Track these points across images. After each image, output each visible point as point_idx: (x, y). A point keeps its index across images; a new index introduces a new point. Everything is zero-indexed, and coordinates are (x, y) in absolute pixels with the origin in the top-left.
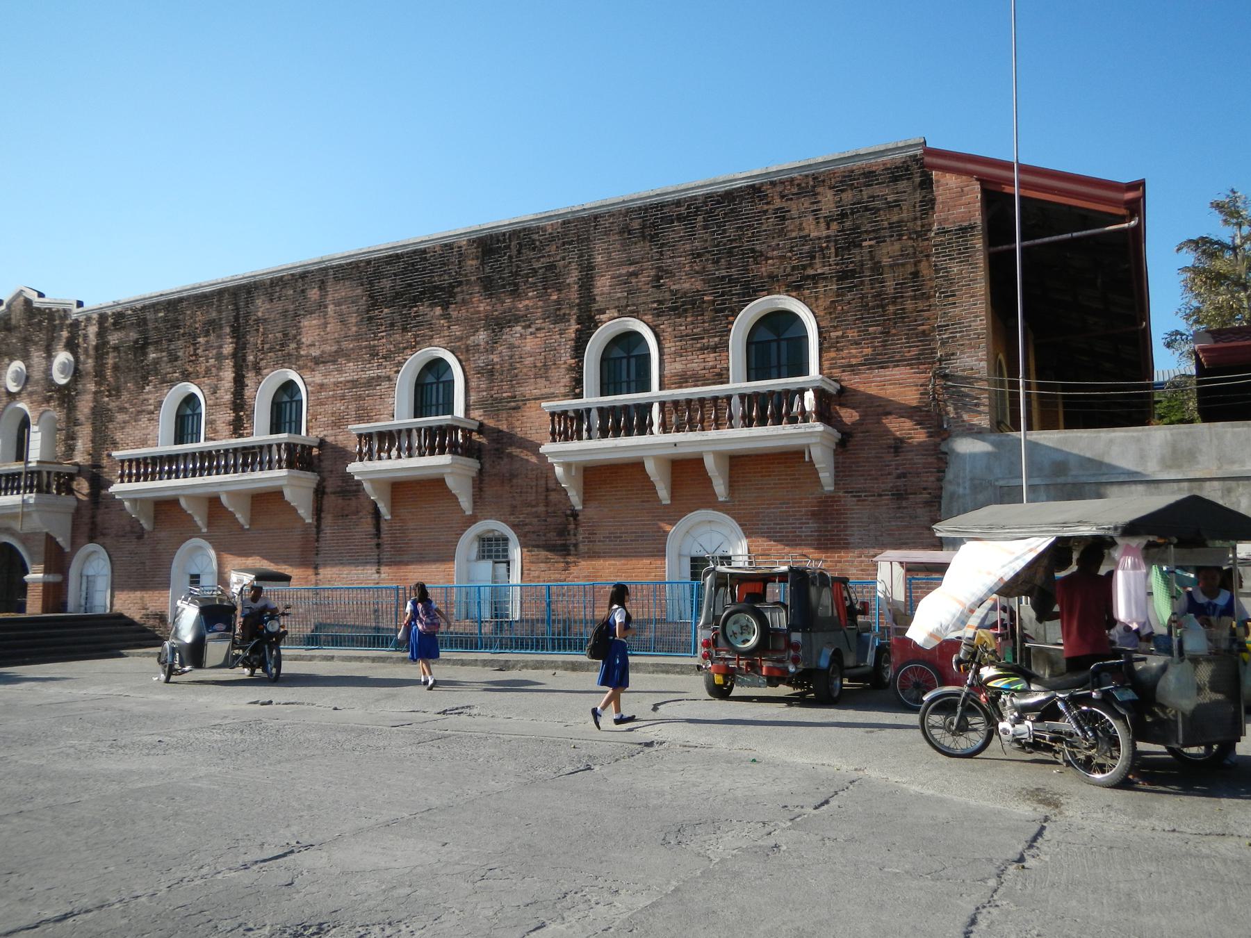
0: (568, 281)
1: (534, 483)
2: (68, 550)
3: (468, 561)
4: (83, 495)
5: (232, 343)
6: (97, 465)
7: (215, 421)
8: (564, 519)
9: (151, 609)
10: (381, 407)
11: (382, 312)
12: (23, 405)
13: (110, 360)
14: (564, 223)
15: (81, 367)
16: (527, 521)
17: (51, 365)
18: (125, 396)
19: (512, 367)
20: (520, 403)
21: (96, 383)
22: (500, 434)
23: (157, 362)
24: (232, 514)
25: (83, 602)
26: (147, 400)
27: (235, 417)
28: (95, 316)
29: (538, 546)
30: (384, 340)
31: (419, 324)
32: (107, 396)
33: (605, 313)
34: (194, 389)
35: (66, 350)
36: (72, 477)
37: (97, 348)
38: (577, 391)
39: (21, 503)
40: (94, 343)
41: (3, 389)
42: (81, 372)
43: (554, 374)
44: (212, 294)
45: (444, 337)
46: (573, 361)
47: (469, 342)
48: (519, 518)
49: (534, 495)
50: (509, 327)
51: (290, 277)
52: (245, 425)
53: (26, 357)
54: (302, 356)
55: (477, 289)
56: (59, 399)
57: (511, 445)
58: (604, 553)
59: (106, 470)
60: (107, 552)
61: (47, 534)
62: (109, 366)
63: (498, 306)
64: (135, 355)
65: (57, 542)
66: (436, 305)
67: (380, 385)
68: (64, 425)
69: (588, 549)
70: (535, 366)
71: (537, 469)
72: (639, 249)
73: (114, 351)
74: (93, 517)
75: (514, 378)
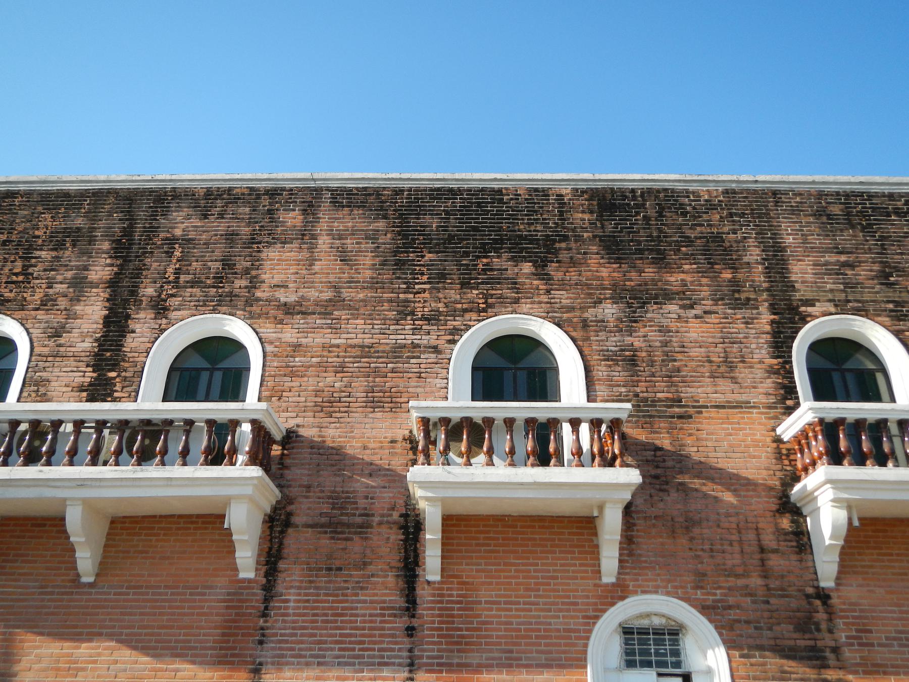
0: (746, 259)
1: (735, 537)
3: (606, 670)
5: (112, 265)
7: (48, 381)
8: (804, 603)
10: (419, 390)
11: (423, 257)
14: (726, 192)
16: (731, 600)
19: (669, 357)
20: (691, 410)
22: (659, 453)
24: (71, 550)
27: (96, 379)
29: (761, 648)
30: (427, 295)
31: (498, 281)
33: (814, 305)
38: (790, 403)
43: (742, 373)
44: (83, 195)
45: (540, 303)
46: (775, 361)
47: (586, 315)
48: (715, 594)
49: (737, 556)
50: (655, 303)
51: (246, 192)
52: (116, 394)
54: (258, 300)
55: (594, 249)
57: (681, 472)
58: (893, 666)
63: (633, 275)
66: (525, 259)
67: (419, 357)
69: (862, 658)
70: (710, 362)
71: (737, 514)
72: (846, 238)
75: (672, 376)
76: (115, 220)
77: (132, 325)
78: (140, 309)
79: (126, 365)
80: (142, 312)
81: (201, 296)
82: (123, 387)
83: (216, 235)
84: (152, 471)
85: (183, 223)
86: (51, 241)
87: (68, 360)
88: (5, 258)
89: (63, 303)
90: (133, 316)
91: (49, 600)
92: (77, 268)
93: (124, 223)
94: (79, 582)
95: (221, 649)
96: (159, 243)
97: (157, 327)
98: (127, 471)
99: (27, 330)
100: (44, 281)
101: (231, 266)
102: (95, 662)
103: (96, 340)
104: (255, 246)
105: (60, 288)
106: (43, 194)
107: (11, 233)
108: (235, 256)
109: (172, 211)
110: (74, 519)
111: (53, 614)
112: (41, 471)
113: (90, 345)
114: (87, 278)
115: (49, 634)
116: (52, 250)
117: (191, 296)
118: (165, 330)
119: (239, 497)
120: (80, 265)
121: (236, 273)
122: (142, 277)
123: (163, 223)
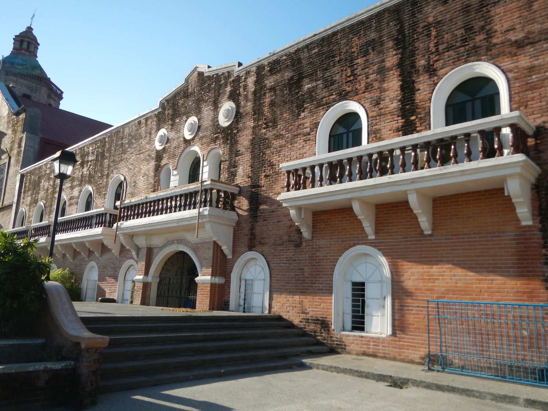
2: (230, 257)
4: (244, 210)
5: (397, 54)
6: (255, 185)
7: (380, 130)
9: (310, 314)
12: (196, 148)
13: (267, 100)
15: (241, 110)
17: (218, 114)
18: (281, 125)
21: (254, 120)
23: (311, 91)
24: (415, 218)
25: (242, 303)
26: (303, 124)
27: (404, 123)
28: (254, 69)
32: (264, 128)
34: (354, 106)
35: (229, 100)
36: (234, 197)
37: (255, 93)
39: (197, 215)
40: (253, 90)
41: (182, 139)
42: (241, 114)
44: (370, 19)
52: (418, 129)
53: (198, 112)
54: (495, 45)
56: (223, 137)
59: (263, 189)
60: (265, 258)
61: (215, 242)
62: (267, 104)
64: (290, 90)
65: (222, 250)
68: (227, 157)
73: (270, 92)
74: (252, 229)
76: (391, 26)
77: (417, 86)
78: (419, 75)
79: (419, 110)
80: (421, 76)
81: (455, 55)
82: (421, 124)
83: (456, 12)
84: (451, 168)
85: (432, 12)
86: (361, 52)
87: (387, 116)
88: (341, 70)
89: (376, 85)
90: (416, 81)
91: (410, 245)
92: (379, 62)
93: (397, 27)
94: (423, 234)
95: (519, 268)
96: (421, 30)
97: (432, 83)
98: (436, 170)
99: (362, 105)
100: (363, 76)
101: (471, 29)
102: (443, 275)
103: (399, 101)
104: (484, 9)
105: (372, 77)
106: (350, 27)
107: (340, 55)
108: (472, 21)
109: (424, 8)
110: (413, 200)
111: (414, 251)
112: (390, 178)
113: (396, 104)
114: (385, 66)
115: (415, 262)
116: (363, 57)
117: (448, 57)
118: (437, 83)
119: (512, 176)
120: (380, 60)
121: (475, 32)
122: (416, 55)
123: (421, 17)
